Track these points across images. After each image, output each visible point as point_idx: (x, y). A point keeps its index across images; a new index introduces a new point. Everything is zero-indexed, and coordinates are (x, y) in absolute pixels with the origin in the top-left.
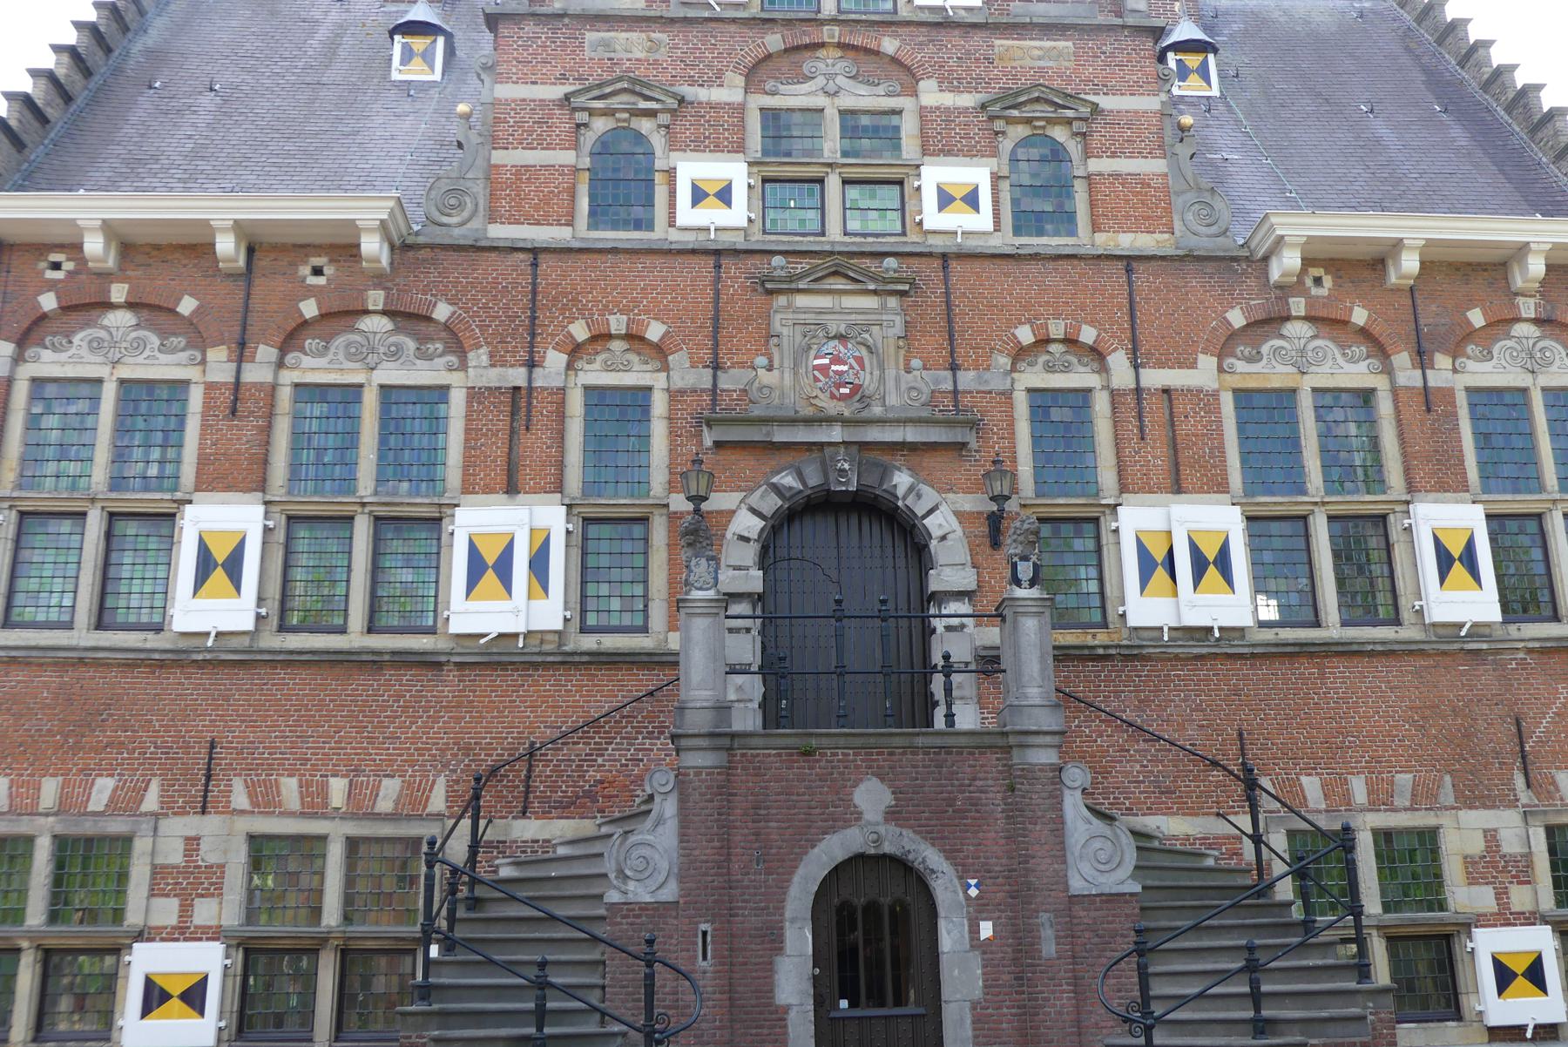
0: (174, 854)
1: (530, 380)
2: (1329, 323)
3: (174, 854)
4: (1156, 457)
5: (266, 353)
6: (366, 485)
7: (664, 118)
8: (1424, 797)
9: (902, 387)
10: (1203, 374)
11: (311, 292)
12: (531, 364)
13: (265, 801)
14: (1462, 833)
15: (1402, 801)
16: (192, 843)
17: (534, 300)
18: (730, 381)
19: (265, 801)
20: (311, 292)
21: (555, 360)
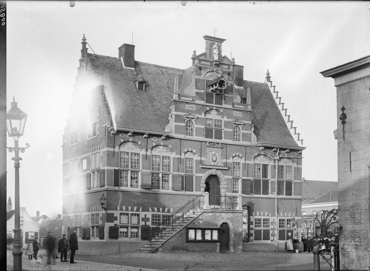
0: (144, 217)
1: (180, 157)
2: (265, 155)
3: (144, 217)
4: (246, 172)
5: (149, 150)
6: (161, 171)
7: (195, 119)
8: (268, 215)
9: (220, 162)
10: (251, 162)
11: (154, 142)
12: (181, 155)
13: (153, 210)
14: (271, 219)
15: (266, 215)
16: (145, 215)
17: (181, 145)
18: (203, 159)
19: (153, 210)
20: (154, 142)
21: (183, 154)
